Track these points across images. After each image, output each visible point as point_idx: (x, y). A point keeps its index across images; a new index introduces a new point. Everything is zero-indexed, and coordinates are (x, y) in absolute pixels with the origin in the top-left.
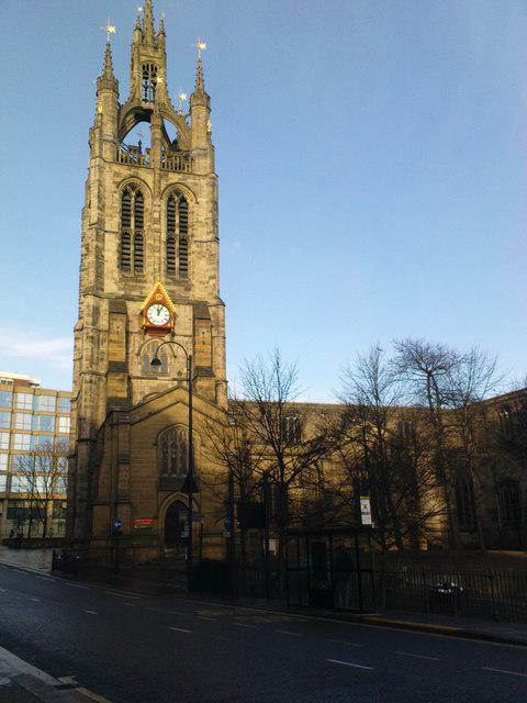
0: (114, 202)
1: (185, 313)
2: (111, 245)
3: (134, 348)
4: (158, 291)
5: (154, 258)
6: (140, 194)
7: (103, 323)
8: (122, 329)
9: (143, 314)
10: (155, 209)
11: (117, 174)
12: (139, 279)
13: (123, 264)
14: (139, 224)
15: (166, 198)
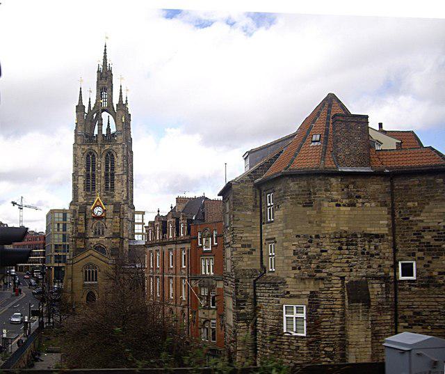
0: (83, 162)
1: (110, 208)
2: (81, 180)
3: (90, 225)
4: (98, 200)
5: (100, 183)
6: (94, 156)
7: (77, 215)
8: (83, 219)
9: (92, 211)
10: (100, 162)
11: (83, 149)
12: (93, 196)
13: (87, 188)
14: (93, 170)
15: (104, 156)
